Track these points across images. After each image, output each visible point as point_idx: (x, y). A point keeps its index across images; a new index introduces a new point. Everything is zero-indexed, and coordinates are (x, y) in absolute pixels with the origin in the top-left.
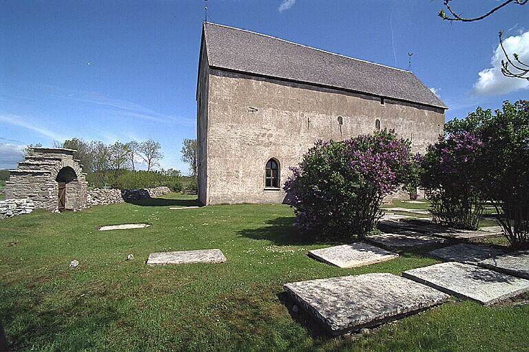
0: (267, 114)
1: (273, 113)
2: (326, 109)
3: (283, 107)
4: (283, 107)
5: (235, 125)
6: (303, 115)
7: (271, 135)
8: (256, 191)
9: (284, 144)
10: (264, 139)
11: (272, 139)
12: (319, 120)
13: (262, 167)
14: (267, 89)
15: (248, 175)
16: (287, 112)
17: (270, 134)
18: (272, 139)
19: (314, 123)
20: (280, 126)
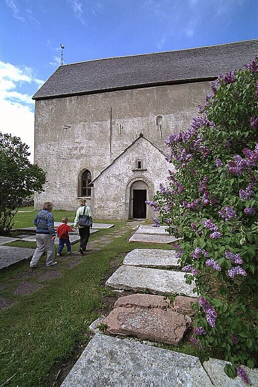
0: (78, 129)
1: (84, 126)
2: (140, 111)
3: (93, 119)
4: (93, 119)
5: (52, 143)
7: (82, 148)
8: (70, 200)
9: (95, 154)
10: (75, 152)
11: (83, 152)
12: (132, 125)
13: (75, 178)
15: (64, 185)
16: (97, 123)
17: (81, 147)
18: (83, 152)
19: (128, 129)
20: (90, 138)
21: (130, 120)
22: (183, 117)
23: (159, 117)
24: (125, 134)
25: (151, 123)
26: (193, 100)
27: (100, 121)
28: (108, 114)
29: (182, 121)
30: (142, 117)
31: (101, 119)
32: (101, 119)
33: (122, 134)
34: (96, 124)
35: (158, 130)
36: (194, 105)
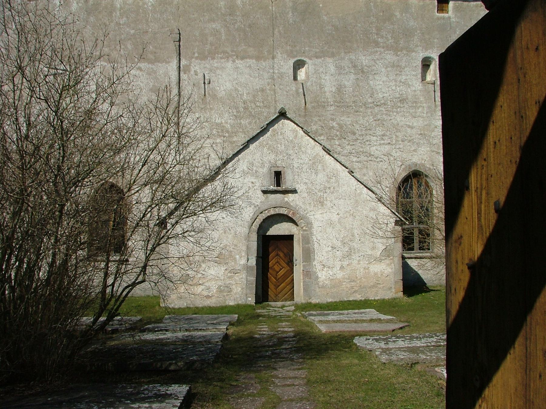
6: (187, 69)
14: (92, 19)
21: (229, 65)
22: (355, 67)
23: (299, 65)
24: (214, 97)
25: (282, 76)
26: (374, 31)
27: (150, 62)
28: (172, 47)
29: (352, 77)
30: (258, 58)
31: (151, 56)
32: (151, 56)
33: (208, 98)
34: (140, 69)
35: (297, 93)
36: (377, 44)
